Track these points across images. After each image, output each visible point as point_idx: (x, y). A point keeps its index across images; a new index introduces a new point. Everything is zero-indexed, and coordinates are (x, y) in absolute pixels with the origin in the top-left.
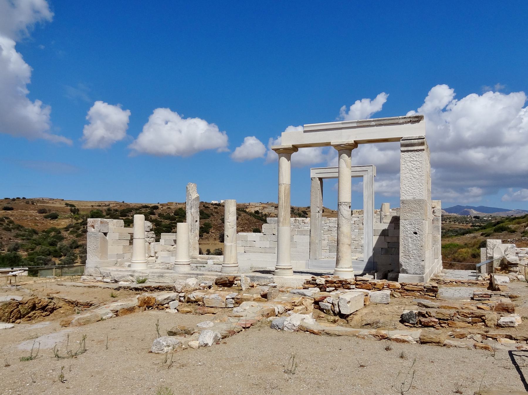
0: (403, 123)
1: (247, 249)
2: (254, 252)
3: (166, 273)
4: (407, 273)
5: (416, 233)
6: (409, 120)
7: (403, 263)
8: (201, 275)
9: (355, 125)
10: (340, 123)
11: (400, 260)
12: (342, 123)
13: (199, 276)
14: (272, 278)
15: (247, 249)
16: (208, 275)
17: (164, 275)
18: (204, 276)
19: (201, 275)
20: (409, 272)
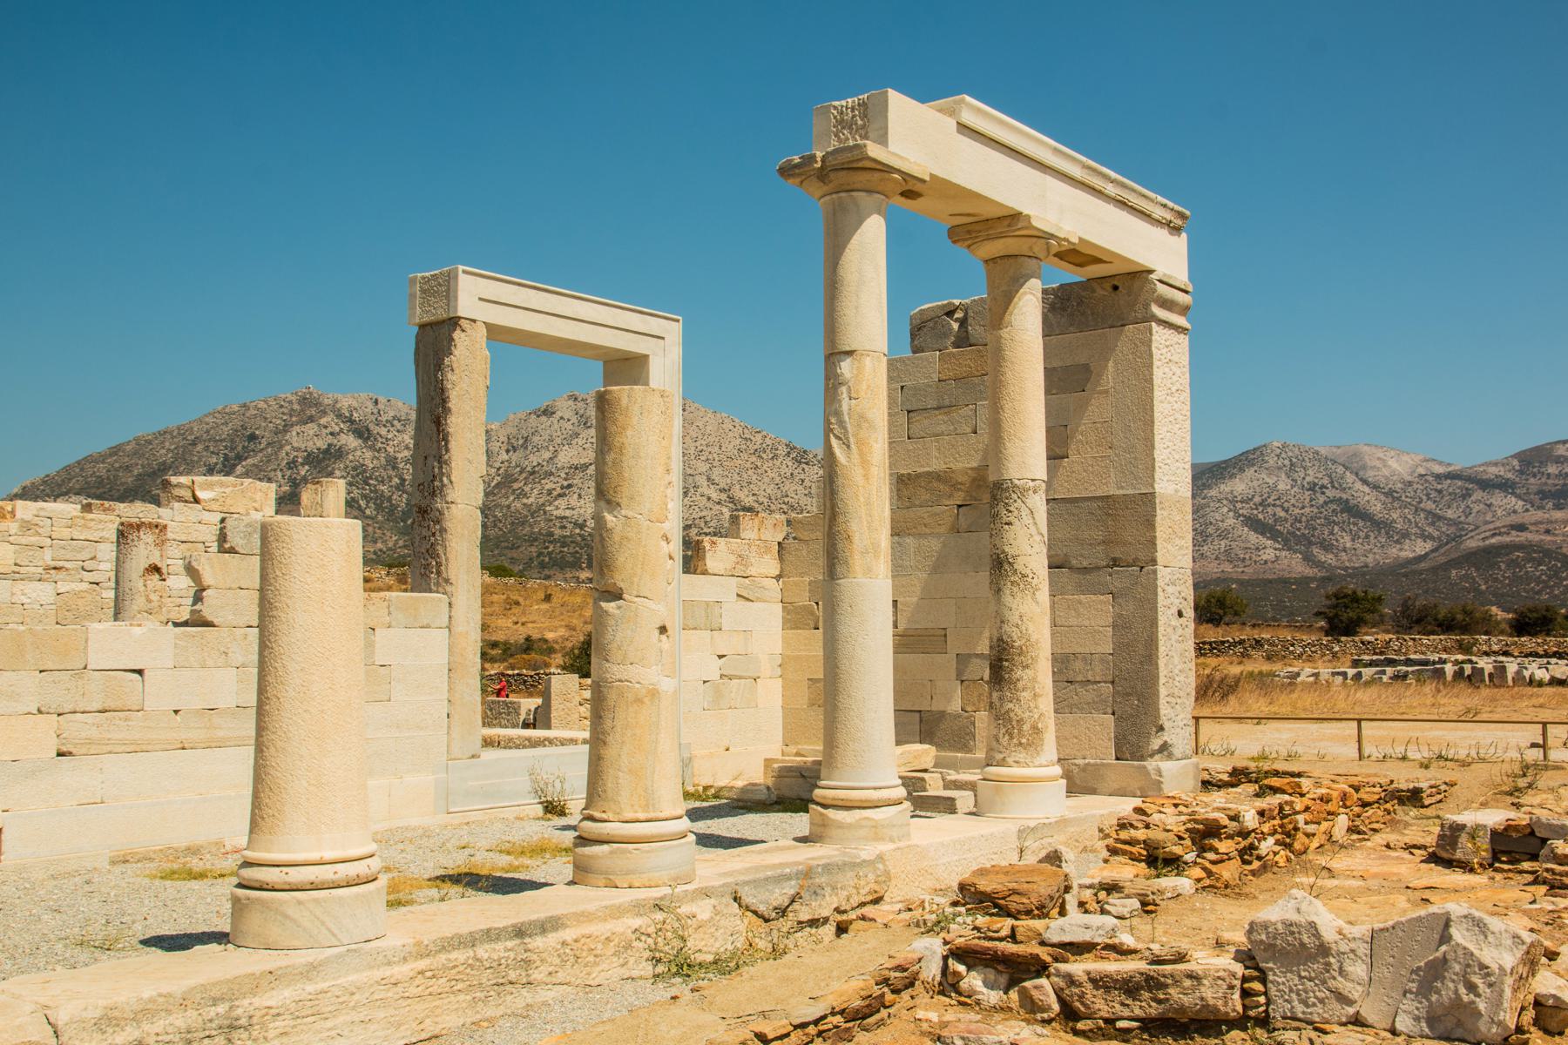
0: (1158, 223)
1: (80, 728)
2: (137, 749)
3: (256, 984)
4: (1170, 756)
5: (1180, 614)
6: (1169, 216)
7: (1167, 725)
8: (545, 927)
9: (1076, 172)
10: (1049, 146)
11: (1162, 712)
12: (1056, 150)
13: (538, 942)
14: (880, 858)
15: (80, 728)
16: (584, 917)
17: (244, 1006)
18: (568, 934)
19: (545, 927)
20: (1177, 752)
